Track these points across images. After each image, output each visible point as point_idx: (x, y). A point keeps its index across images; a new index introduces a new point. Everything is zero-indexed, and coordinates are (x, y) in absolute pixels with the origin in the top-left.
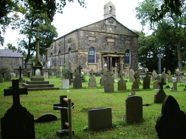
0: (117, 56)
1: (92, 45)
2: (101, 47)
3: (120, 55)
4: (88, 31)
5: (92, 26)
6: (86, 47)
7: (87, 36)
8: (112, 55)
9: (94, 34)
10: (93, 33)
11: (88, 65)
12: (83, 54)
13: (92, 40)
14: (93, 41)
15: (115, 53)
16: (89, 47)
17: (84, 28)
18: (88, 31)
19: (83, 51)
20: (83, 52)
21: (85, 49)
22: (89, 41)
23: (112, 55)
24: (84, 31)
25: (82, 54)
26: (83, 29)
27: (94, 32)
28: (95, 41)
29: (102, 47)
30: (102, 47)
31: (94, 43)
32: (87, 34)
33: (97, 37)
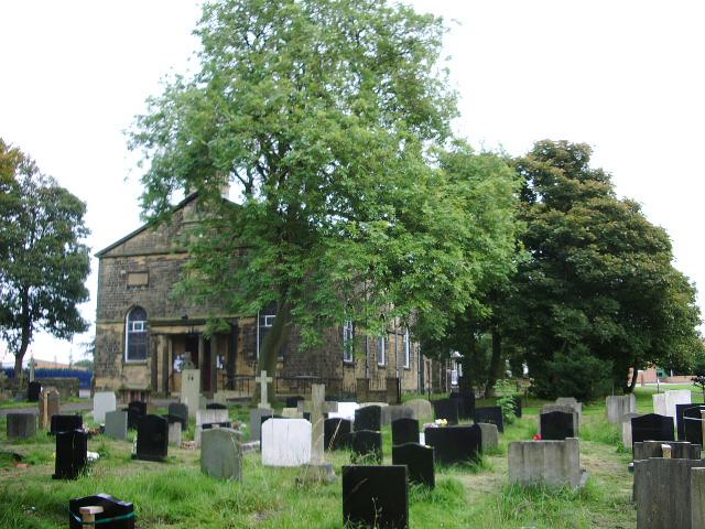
0: (186, 330)
1: (138, 298)
2: (164, 303)
3: (195, 328)
4: (127, 256)
5: (140, 237)
6: (117, 308)
7: (123, 272)
8: (167, 330)
9: (143, 263)
10: (140, 261)
11: (124, 365)
12: (109, 332)
13: (137, 283)
14: (139, 286)
15: (185, 322)
16: (126, 307)
17: (116, 249)
18: (127, 256)
19: (108, 323)
20: (109, 326)
21: (114, 314)
22: (128, 287)
23: (167, 330)
24: (115, 257)
25: (106, 330)
26: (112, 252)
27: (144, 257)
28: (147, 286)
29: (168, 303)
30: (168, 303)
31: (144, 294)
32: (123, 268)
33: (155, 272)
